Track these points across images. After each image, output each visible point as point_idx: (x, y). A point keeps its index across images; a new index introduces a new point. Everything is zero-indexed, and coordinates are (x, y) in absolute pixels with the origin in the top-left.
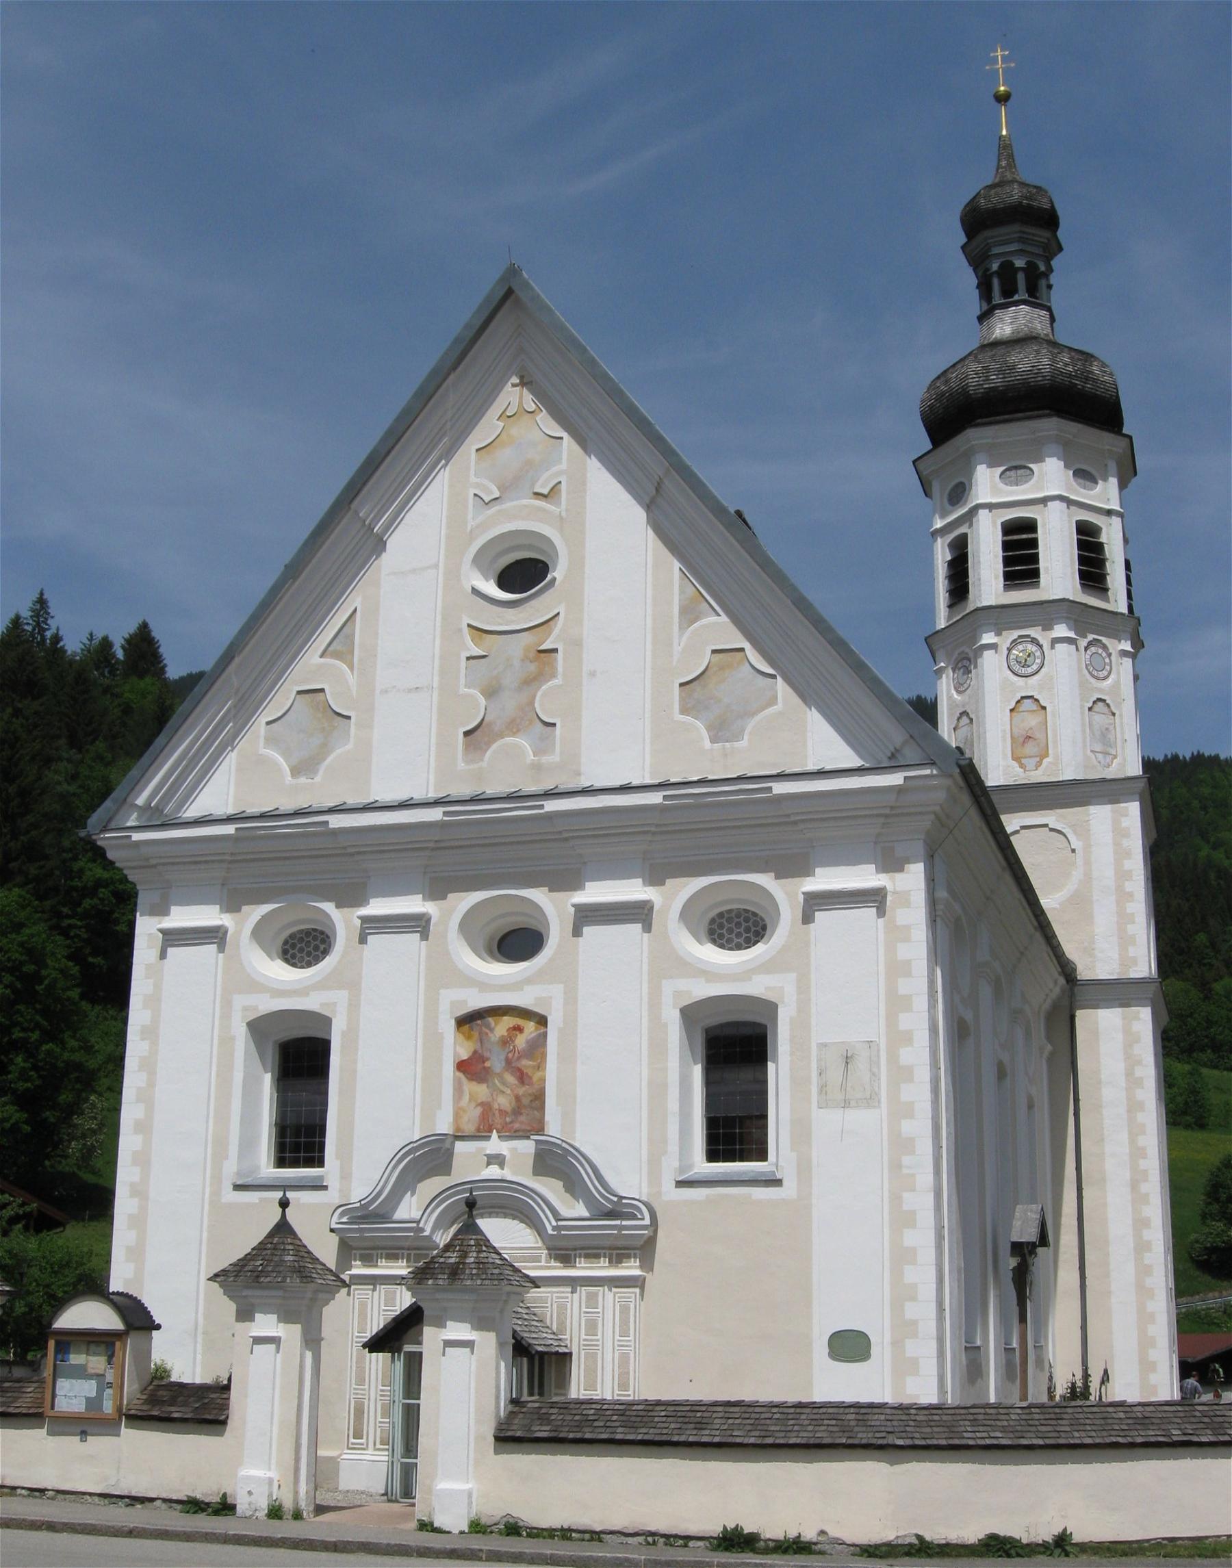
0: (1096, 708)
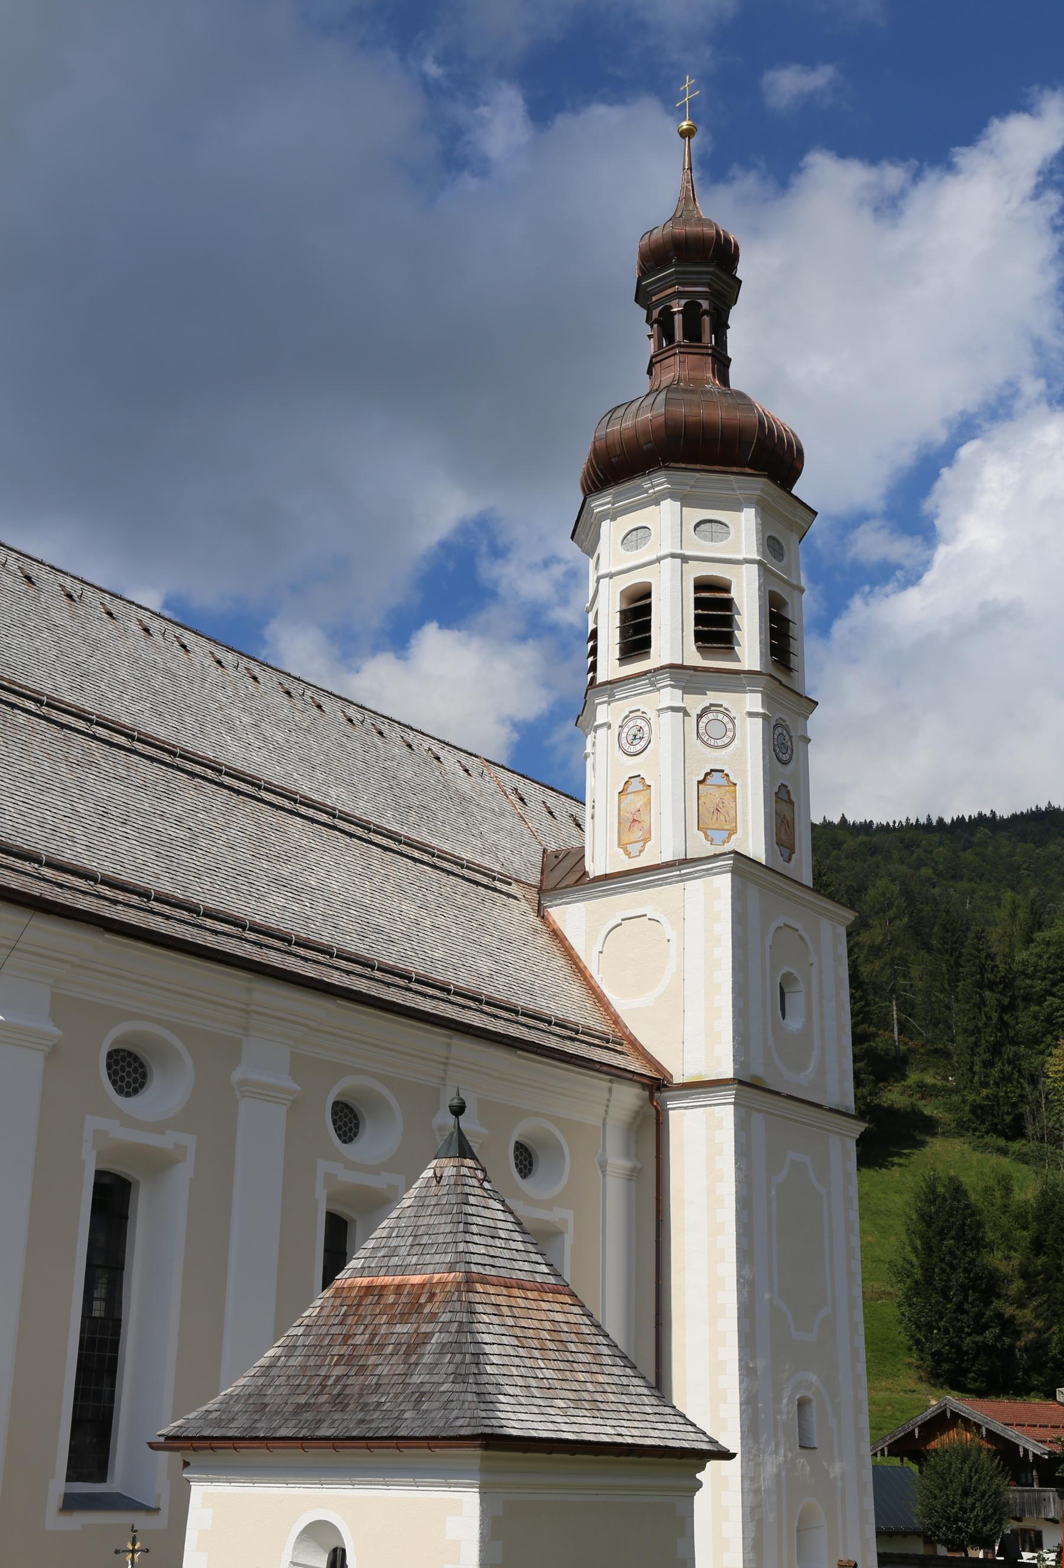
0: (709, 781)
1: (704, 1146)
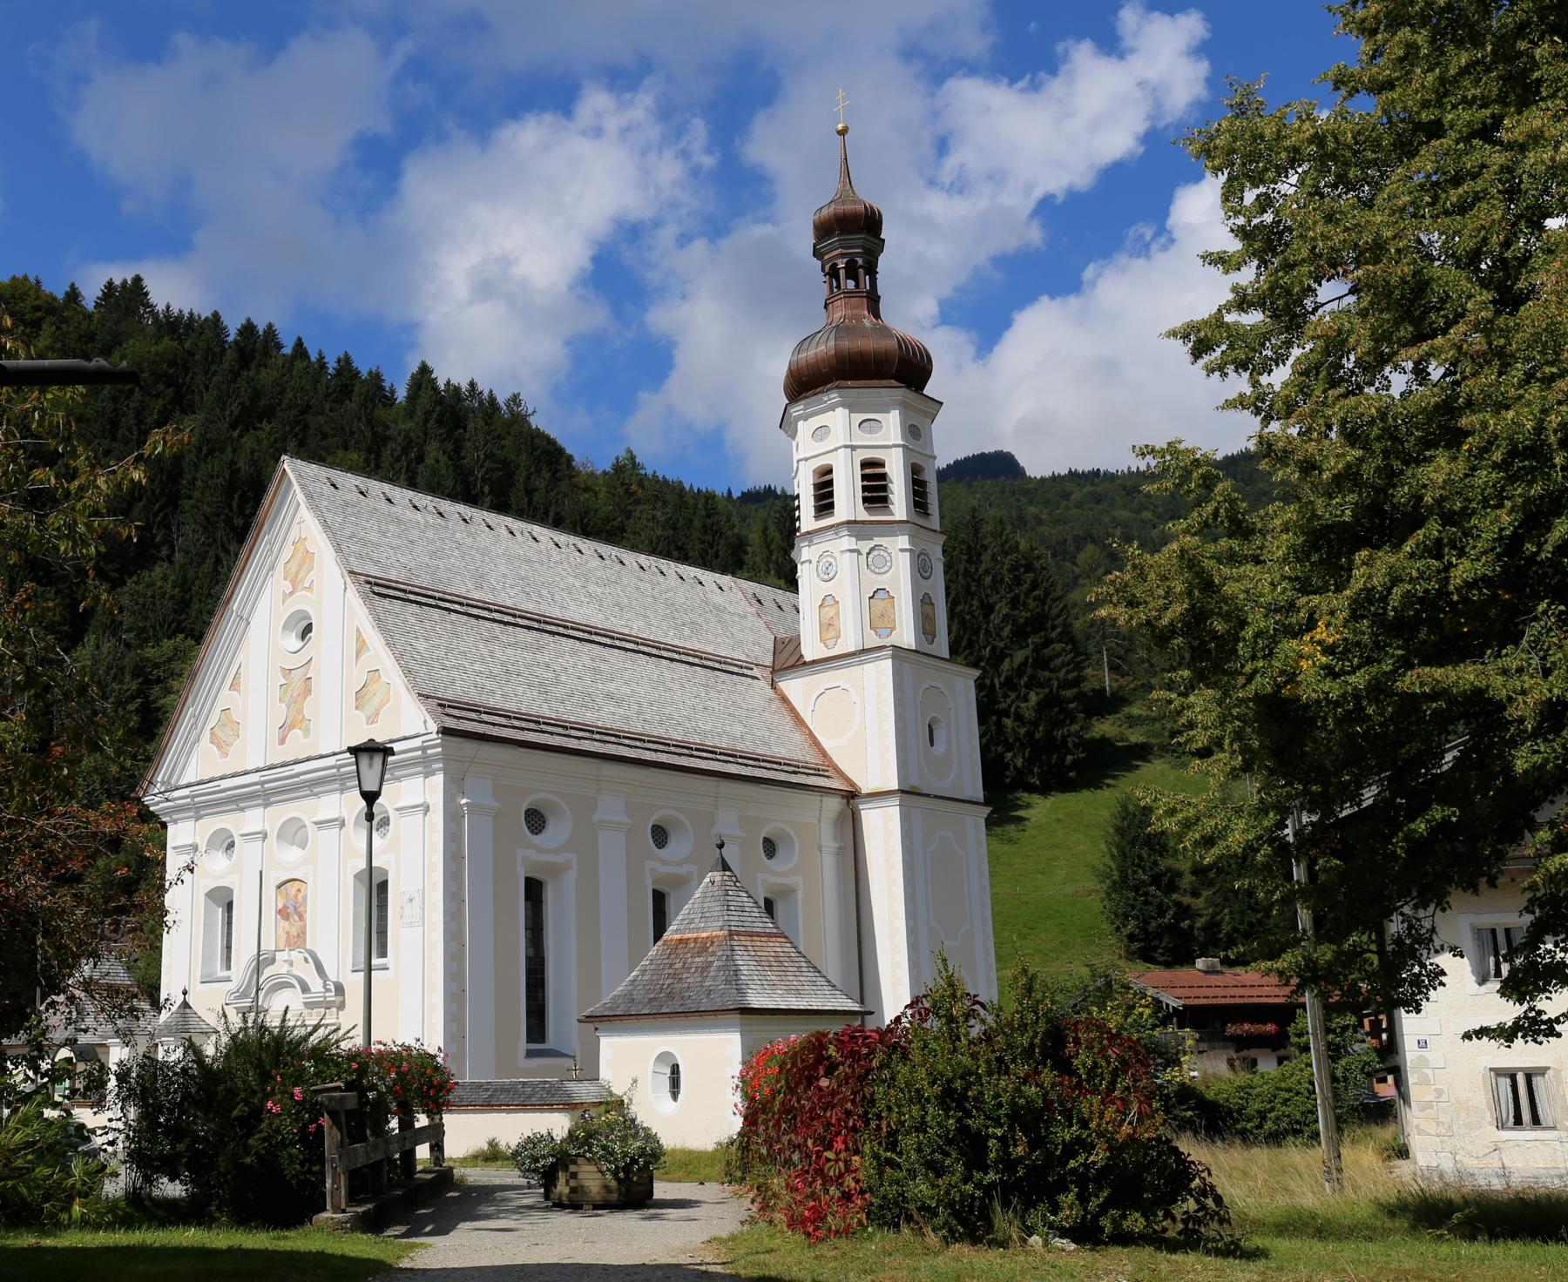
1: (882, 831)
